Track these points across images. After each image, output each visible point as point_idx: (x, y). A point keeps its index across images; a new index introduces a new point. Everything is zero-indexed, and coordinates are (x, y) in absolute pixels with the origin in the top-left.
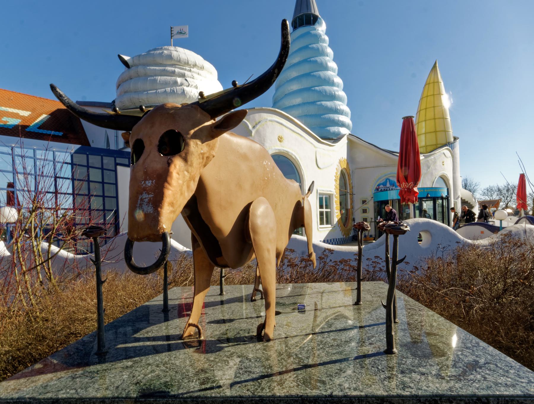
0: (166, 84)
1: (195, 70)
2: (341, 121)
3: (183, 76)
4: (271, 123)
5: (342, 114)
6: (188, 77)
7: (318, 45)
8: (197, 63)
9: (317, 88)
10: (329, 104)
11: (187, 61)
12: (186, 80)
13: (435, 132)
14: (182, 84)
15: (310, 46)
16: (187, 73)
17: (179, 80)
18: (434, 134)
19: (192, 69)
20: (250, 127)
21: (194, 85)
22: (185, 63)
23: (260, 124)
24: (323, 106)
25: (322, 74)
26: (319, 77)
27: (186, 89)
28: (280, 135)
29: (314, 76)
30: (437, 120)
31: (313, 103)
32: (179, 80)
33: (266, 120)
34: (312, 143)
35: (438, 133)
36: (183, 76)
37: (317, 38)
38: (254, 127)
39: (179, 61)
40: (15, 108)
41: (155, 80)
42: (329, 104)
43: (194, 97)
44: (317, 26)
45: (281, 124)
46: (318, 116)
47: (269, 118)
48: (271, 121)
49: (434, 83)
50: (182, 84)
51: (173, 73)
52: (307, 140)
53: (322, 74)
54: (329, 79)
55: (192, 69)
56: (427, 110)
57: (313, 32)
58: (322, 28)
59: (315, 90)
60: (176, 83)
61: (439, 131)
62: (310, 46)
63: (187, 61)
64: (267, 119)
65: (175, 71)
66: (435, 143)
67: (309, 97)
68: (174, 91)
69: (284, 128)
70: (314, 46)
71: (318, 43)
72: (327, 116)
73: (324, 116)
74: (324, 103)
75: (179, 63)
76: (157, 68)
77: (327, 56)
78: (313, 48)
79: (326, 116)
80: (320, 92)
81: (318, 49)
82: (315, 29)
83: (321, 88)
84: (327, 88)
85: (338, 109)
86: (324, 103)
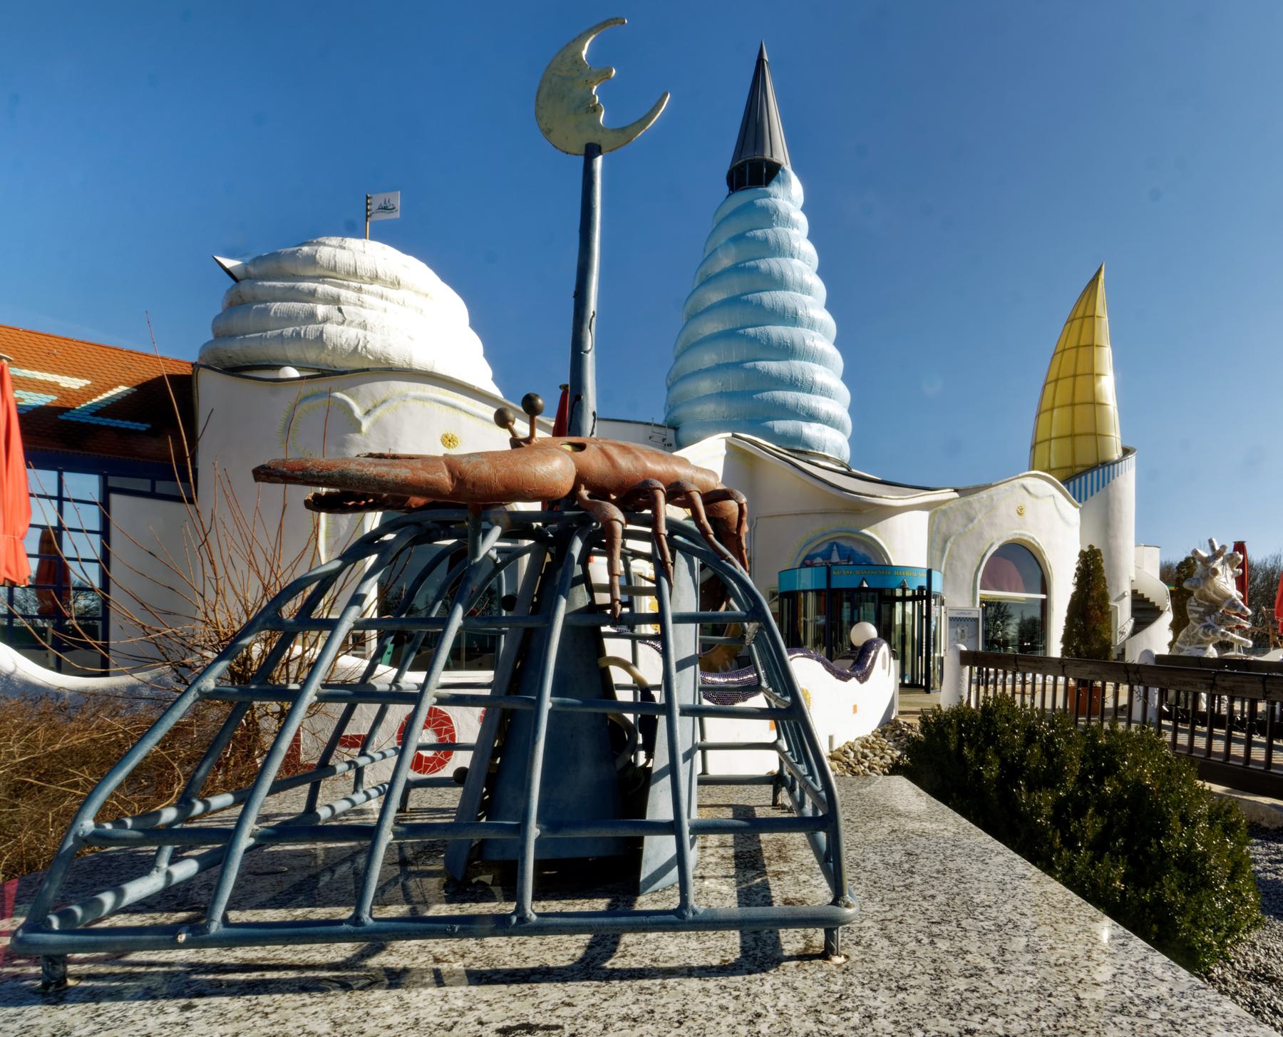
0: (290, 318)
2: (803, 408)
3: (335, 301)
5: (810, 392)
6: (349, 303)
7: (769, 231)
9: (751, 331)
10: (774, 367)
11: (352, 269)
12: (340, 310)
13: (1073, 436)
14: (326, 320)
15: (748, 234)
16: (344, 293)
17: (321, 310)
18: (1068, 442)
20: (358, 412)
22: (348, 273)
23: (384, 406)
25: (768, 297)
26: (760, 305)
27: (330, 329)
29: (748, 302)
30: (1077, 408)
31: (738, 365)
32: (321, 310)
35: (1078, 439)
36: (335, 301)
37: (770, 216)
39: (334, 269)
40: (54, 371)
41: (267, 310)
42: (774, 367)
43: (346, 346)
44: (774, 188)
45: (454, 407)
46: (743, 395)
48: (416, 398)
49: (1083, 317)
50: (326, 320)
51: (311, 296)
53: (768, 297)
54: (784, 309)
55: (364, 286)
56: (1060, 382)
57: (762, 202)
58: (790, 195)
59: (746, 336)
60: (311, 317)
61: (1081, 435)
62: (748, 234)
63: (352, 269)
64: (407, 396)
65: (315, 290)
66: (1068, 463)
67: (734, 353)
68: (298, 334)
69: (463, 416)
70: (759, 233)
71: (771, 227)
72: (767, 395)
73: (759, 396)
74: (762, 365)
75: (333, 274)
76: (278, 284)
77: (792, 256)
78: (754, 238)
79: (765, 394)
80: (754, 340)
81: (766, 240)
82: (768, 195)
83: (759, 330)
84: (777, 331)
85: (797, 380)
86: (762, 365)
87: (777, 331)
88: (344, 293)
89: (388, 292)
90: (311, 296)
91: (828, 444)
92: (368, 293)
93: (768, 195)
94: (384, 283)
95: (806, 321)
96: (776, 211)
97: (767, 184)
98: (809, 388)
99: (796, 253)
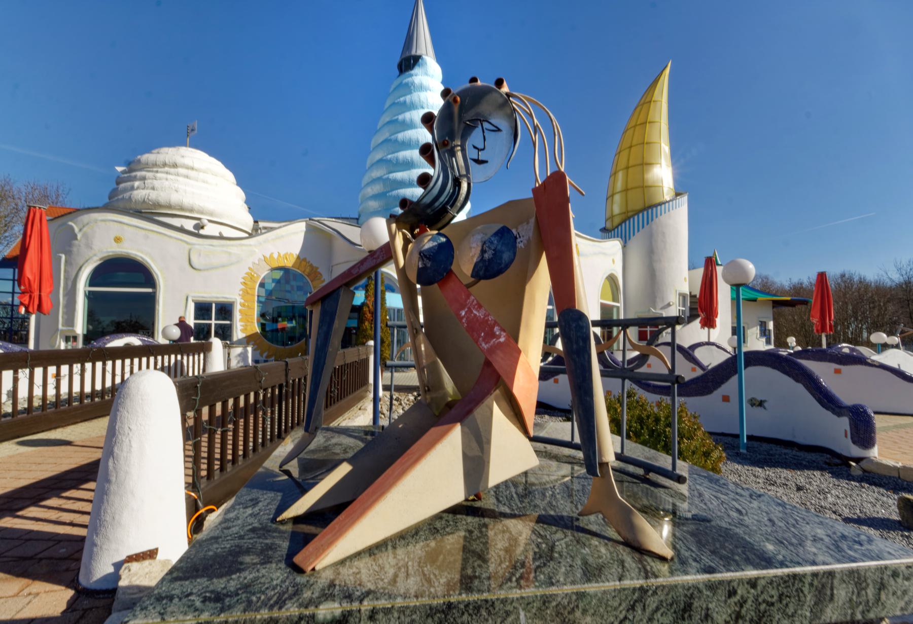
1: (166, 169)
4: (103, 223)
8: (167, 162)
9: (389, 156)
10: (399, 175)
19: (160, 170)
21: (151, 186)
26: (396, 141)
28: (118, 235)
29: (390, 140)
33: (96, 221)
34: (181, 240)
38: (80, 230)
44: (416, 70)
47: (100, 218)
52: (170, 237)
53: (400, 136)
54: (410, 140)
70: (402, 99)
71: (410, 93)
72: (394, 193)
74: (392, 176)
80: (390, 161)
86: (392, 176)
88: (148, 175)
89: (172, 170)
90: (135, 179)
92: (161, 172)
93: (412, 75)
94: (170, 166)
96: (413, 83)
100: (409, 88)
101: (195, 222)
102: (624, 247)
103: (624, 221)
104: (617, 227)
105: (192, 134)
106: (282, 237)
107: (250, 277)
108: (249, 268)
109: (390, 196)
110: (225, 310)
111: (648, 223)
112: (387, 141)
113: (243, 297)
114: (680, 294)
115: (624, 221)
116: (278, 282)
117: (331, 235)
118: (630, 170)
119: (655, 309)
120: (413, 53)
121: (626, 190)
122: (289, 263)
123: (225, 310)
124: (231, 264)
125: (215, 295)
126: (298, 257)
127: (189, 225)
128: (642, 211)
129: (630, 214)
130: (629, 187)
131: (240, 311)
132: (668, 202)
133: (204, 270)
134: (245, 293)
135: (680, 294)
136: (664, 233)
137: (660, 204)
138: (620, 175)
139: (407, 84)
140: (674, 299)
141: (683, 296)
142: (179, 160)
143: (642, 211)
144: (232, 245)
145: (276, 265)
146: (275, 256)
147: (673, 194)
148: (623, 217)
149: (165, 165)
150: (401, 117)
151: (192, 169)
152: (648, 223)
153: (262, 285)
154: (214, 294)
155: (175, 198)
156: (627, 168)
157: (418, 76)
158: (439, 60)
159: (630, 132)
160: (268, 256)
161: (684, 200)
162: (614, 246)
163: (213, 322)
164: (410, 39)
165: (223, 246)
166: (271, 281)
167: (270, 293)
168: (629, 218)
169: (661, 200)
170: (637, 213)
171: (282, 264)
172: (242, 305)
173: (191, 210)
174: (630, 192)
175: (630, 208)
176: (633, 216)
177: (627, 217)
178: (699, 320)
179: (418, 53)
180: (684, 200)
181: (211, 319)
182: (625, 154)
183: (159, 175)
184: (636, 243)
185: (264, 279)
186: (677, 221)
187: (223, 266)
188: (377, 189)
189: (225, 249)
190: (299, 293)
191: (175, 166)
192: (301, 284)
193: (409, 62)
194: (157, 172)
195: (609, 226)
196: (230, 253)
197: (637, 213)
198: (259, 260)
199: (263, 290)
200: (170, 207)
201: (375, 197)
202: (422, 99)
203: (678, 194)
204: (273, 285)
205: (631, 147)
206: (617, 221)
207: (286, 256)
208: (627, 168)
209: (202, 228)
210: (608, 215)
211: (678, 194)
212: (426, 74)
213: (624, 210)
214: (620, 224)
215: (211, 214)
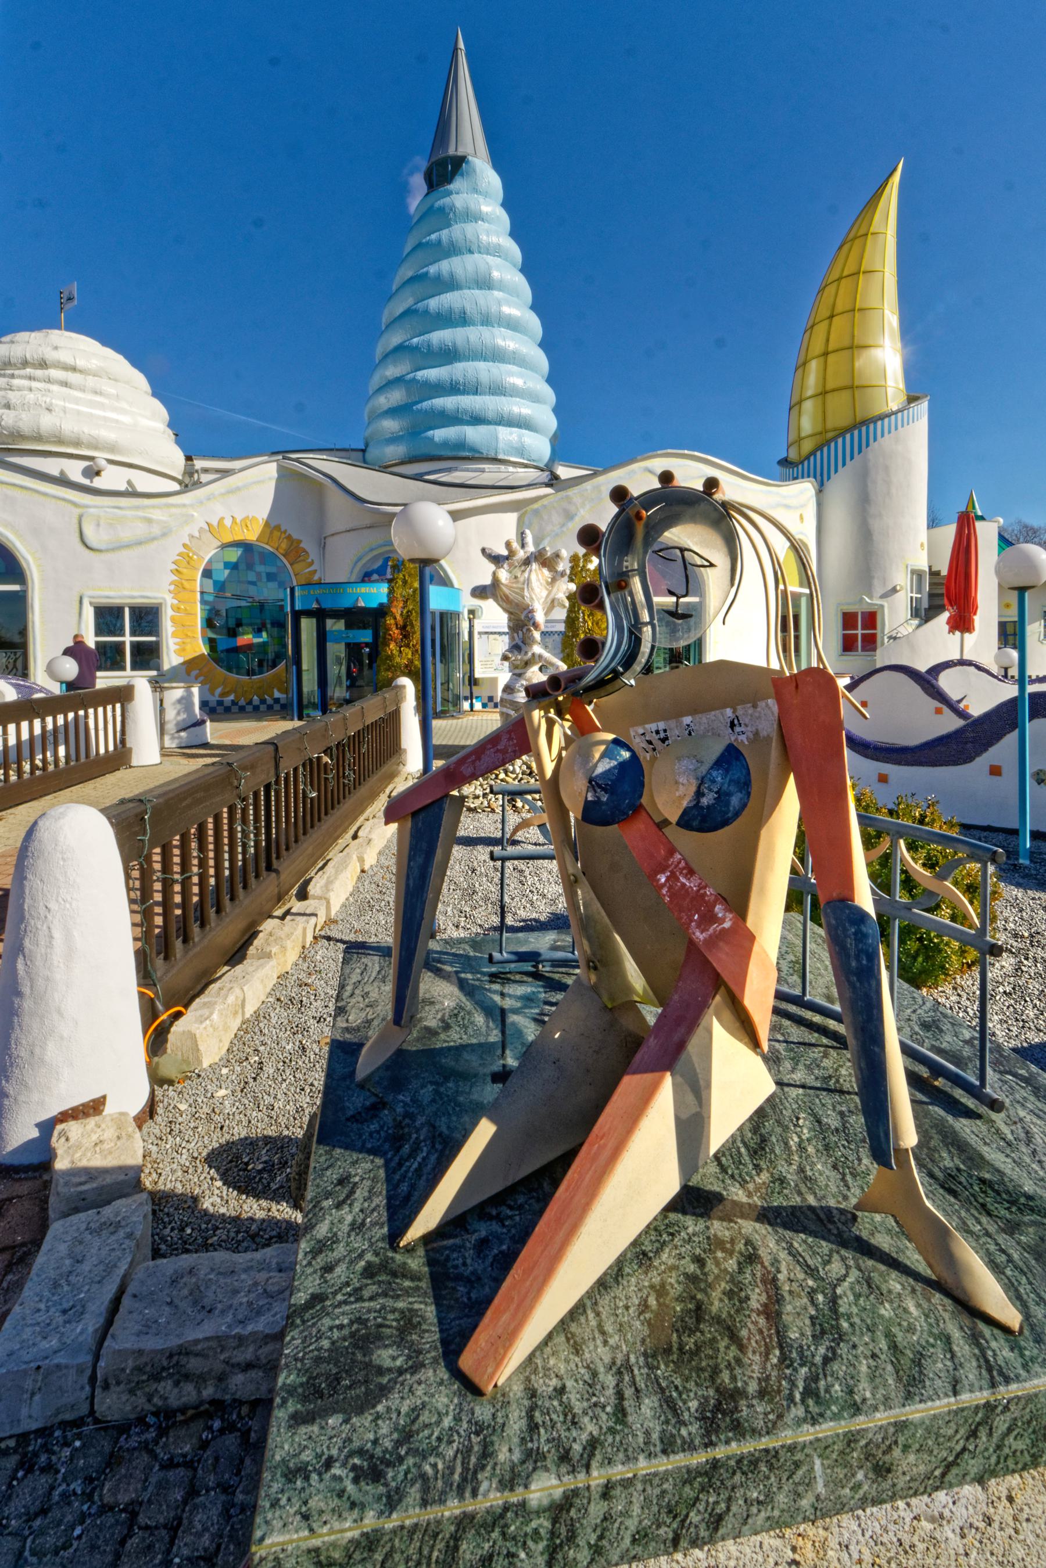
1: (29, 371)
2: (465, 411)
5: (476, 392)
9: (415, 340)
10: (432, 374)
19: (17, 372)
24: (418, 381)
26: (426, 312)
29: (416, 311)
34: (64, 500)
42: (432, 374)
44: (457, 184)
52: (45, 494)
53: (433, 304)
54: (451, 310)
70: (433, 237)
71: (449, 225)
72: (426, 405)
73: (419, 406)
74: (422, 375)
77: (471, 252)
80: (416, 349)
86: (422, 375)
87: (440, 337)
89: (39, 373)
91: (501, 445)
93: (449, 193)
94: (34, 366)
95: (477, 318)
96: (452, 208)
97: (450, 182)
98: (498, 390)
99: (474, 248)
100: (444, 217)
101: (85, 464)
102: (820, 491)
103: (820, 448)
104: (808, 458)
105: (69, 306)
106: (238, 489)
107: (186, 558)
108: (184, 545)
109: (420, 411)
110: (146, 618)
111: (860, 452)
112: (408, 312)
113: (175, 594)
114: (913, 572)
115: (820, 448)
116: (234, 567)
117: (320, 486)
118: (831, 358)
119: (871, 598)
120: (451, 151)
121: (823, 393)
122: (252, 535)
123: (146, 618)
124: (154, 539)
125: (126, 593)
126: (267, 524)
127: (74, 470)
128: (850, 429)
129: (830, 435)
130: (830, 385)
131: (173, 619)
132: (895, 413)
133: (107, 550)
134: (179, 588)
135: (913, 572)
136: (887, 469)
137: (882, 417)
138: (814, 366)
139: (442, 209)
140: (902, 579)
141: (918, 574)
142: (51, 355)
143: (850, 429)
144: (153, 507)
145: (228, 538)
146: (228, 522)
147: (903, 398)
148: (818, 440)
149: (25, 363)
150: (432, 269)
151: (74, 369)
152: (860, 452)
153: (207, 573)
154: (126, 591)
155: (47, 422)
156: (826, 354)
157: (459, 195)
158: (498, 164)
159: (831, 290)
160: (215, 523)
161: (923, 407)
162: (804, 490)
163: (128, 639)
164: (444, 127)
165: (137, 508)
166: (221, 566)
167: (220, 587)
168: (828, 443)
169: (884, 410)
170: (843, 432)
171: (239, 537)
172: (176, 609)
173: (77, 444)
174: (829, 396)
175: (830, 425)
176: (834, 439)
177: (825, 440)
178: (946, 615)
179: (461, 152)
180: (923, 407)
181: (123, 635)
182: (821, 330)
183: (16, 382)
184: (840, 486)
185: (210, 562)
186: (910, 446)
187: (139, 543)
188: (396, 397)
189: (141, 513)
190: (271, 585)
191: (43, 364)
192: (273, 570)
193: (445, 170)
194: (12, 376)
195: (793, 455)
196: (149, 521)
197: (843, 432)
198: (201, 530)
199: (209, 583)
200: (38, 438)
201: (393, 412)
202: (468, 236)
203: (912, 399)
204: (227, 572)
205: (831, 317)
206: (807, 446)
207: (246, 522)
208: (826, 354)
209: (98, 473)
210: (793, 437)
211: (912, 399)
212: (476, 190)
213: (819, 429)
214: (813, 453)
215: (112, 448)
